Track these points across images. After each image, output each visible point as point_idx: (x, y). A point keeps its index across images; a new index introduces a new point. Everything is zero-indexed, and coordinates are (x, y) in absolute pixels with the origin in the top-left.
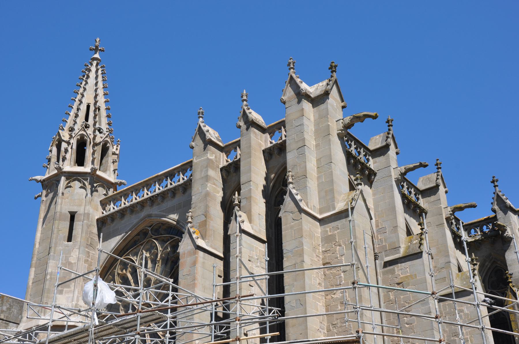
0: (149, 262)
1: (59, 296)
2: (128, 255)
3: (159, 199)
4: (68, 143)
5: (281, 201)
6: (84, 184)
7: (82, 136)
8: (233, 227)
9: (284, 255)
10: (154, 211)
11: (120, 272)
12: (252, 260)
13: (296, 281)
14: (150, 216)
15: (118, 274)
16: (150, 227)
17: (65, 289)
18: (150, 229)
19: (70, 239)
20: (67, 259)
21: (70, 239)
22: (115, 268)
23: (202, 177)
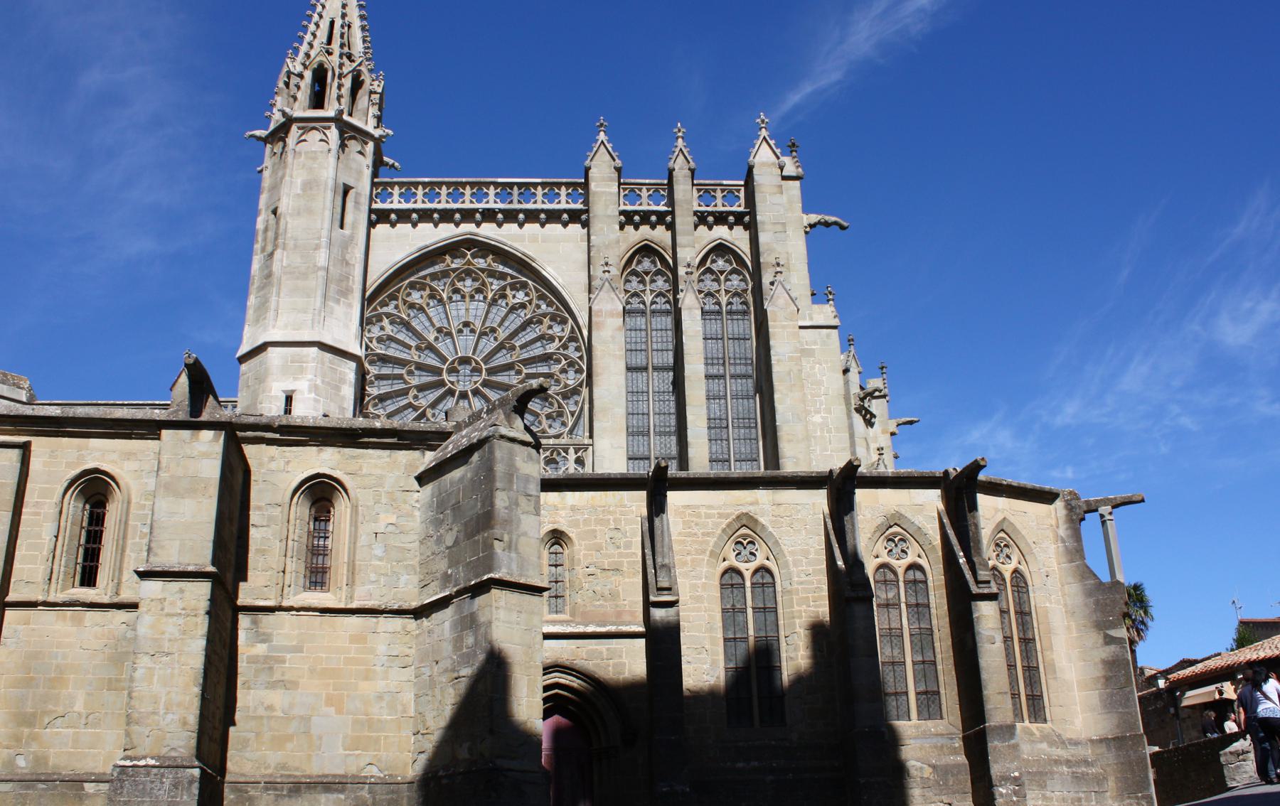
1: (336, 307)
7: (321, 65)
13: (791, 391)
17: (342, 299)
18: (469, 253)
22: (398, 290)
23: (609, 216)
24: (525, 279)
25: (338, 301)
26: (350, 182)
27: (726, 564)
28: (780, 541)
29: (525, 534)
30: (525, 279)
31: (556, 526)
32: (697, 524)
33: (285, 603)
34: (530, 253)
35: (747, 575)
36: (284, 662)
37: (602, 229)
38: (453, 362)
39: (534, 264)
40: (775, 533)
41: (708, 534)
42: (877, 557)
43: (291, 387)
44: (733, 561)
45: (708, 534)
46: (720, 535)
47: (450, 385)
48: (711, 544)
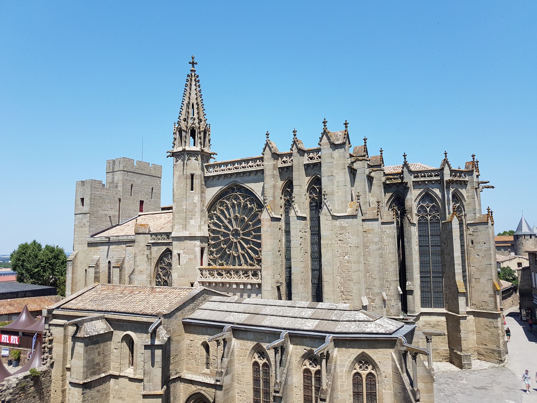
0: (236, 206)
2: (223, 199)
3: (242, 174)
4: (186, 132)
5: (321, 208)
6: (197, 157)
8: (292, 214)
9: (321, 237)
10: (238, 179)
11: (219, 207)
12: (301, 230)
14: (236, 182)
15: (219, 208)
16: (236, 186)
19: (192, 189)
20: (192, 200)
21: (192, 189)
22: (216, 205)
24: (252, 197)
25: (192, 219)
26: (193, 172)
27: (254, 360)
28: (269, 355)
29: (156, 375)
30: (252, 197)
31: (205, 340)
32: (244, 345)
33: (121, 374)
34: (252, 188)
35: (261, 365)
36: (122, 392)
37: (268, 181)
38: (232, 231)
39: (254, 192)
40: (268, 352)
41: (247, 349)
42: (305, 365)
43: (179, 252)
44: (257, 359)
45: (247, 349)
46: (251, 350)
47: (232, 240)
48: (248, 353)
